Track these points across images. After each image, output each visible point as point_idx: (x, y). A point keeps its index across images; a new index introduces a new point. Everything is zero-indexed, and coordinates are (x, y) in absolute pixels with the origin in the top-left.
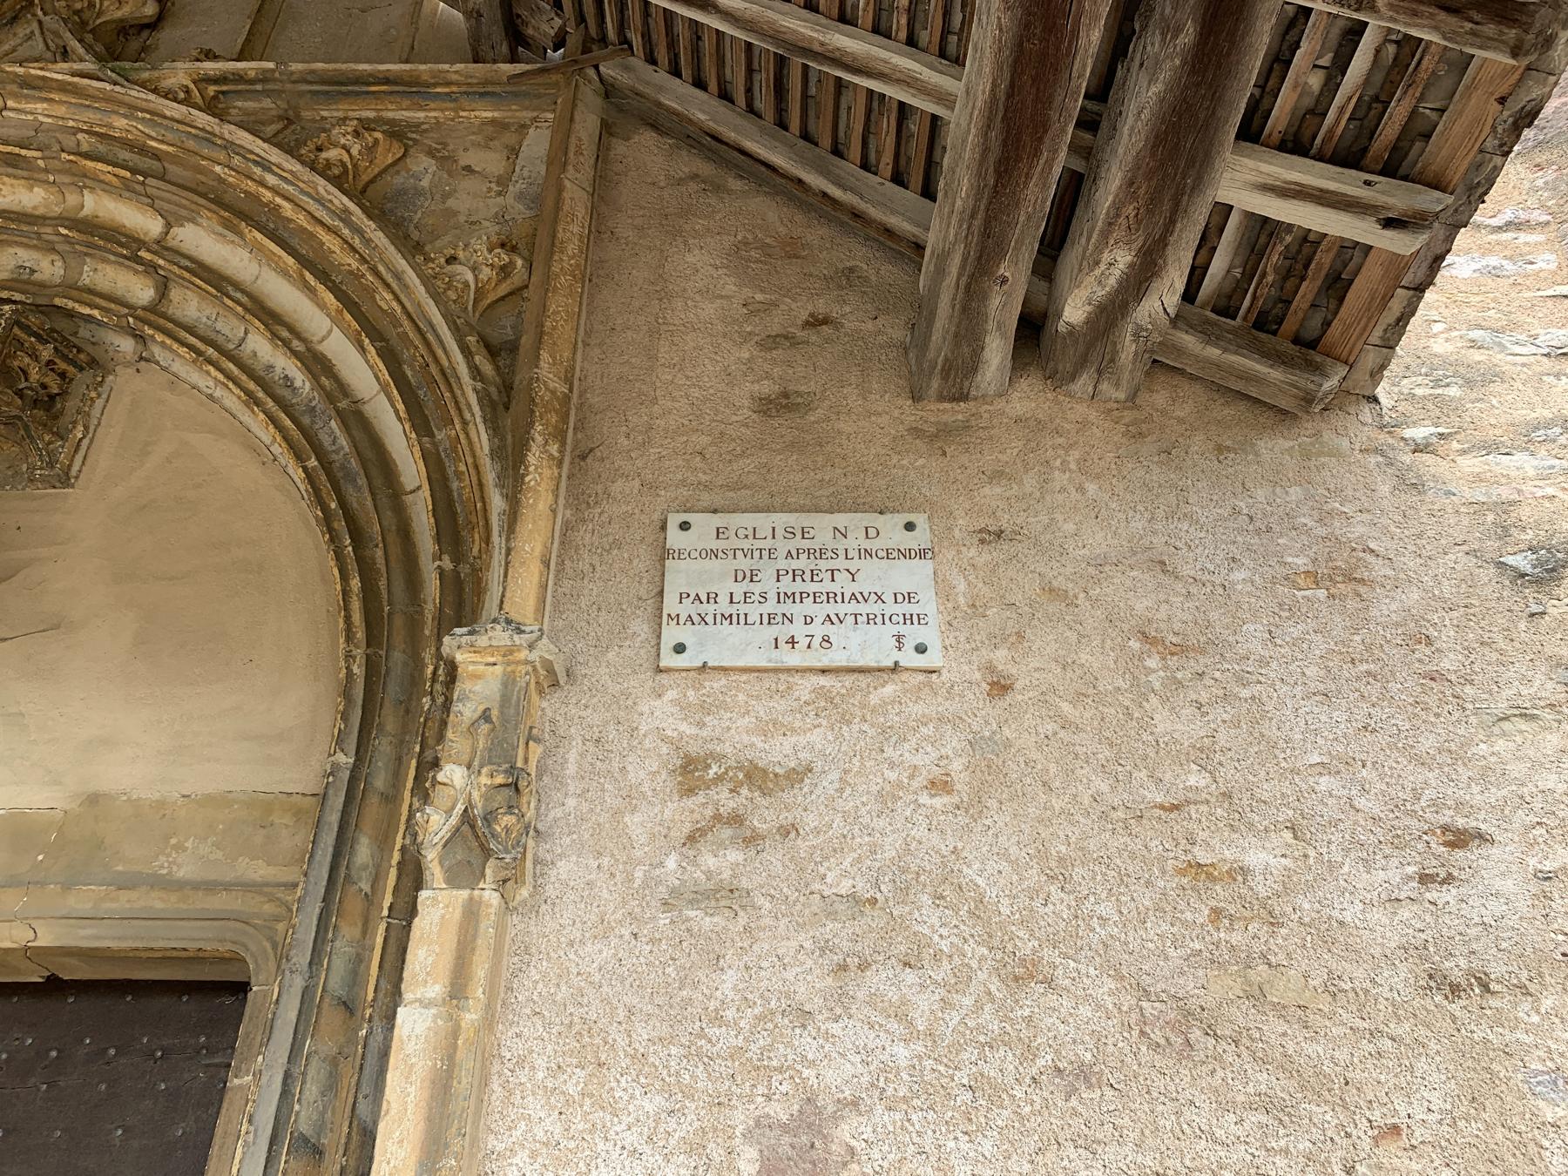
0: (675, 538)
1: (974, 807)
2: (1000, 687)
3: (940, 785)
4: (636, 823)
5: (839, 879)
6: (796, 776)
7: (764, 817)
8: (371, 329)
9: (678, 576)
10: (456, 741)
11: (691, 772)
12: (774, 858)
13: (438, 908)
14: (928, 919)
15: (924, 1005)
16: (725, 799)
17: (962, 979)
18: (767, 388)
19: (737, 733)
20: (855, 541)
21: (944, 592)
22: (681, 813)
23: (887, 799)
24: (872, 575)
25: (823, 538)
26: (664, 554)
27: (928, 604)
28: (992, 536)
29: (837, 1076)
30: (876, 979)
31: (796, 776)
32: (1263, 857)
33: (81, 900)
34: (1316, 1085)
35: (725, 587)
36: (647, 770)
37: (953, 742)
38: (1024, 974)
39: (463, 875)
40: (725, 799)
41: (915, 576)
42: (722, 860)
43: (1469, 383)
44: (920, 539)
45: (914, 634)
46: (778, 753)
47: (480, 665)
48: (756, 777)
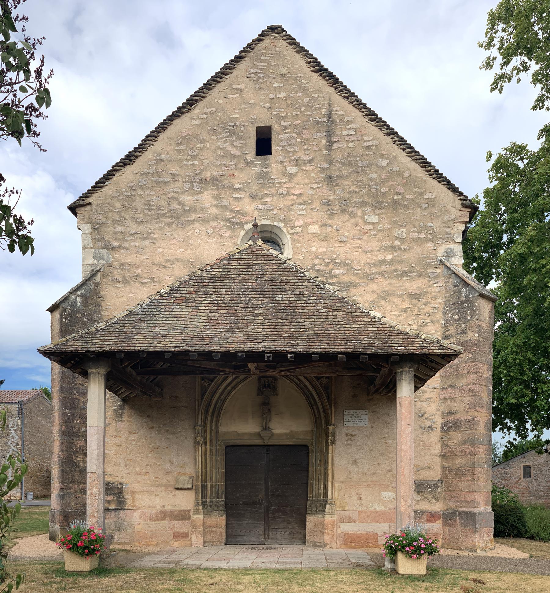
0: (345, 413)
1: (369, 438)
2: (372, 427)
3: (367, 436)
4: (343, 439)
5: (358, 443)
6: (355, 435)
7: (353, 439)
8: (313, 387)
9: (345, 417)
10: (330, 435)
11: (347, 435)
12: (353, 442)
13: (330, 447)
14: (365, 446)
15: (364, 452)
16: (349, 437)
17: (367, 451)
18: (353, 394)
19: (350, 432)
20: (361, 413)
21: (368, 418)
22: (346, 438)
23: (362, 437)
24: (363, 417)
25: (358, 413)
26: (344, 415)
27: (367, 420)
28: (373, 412)
29: (357, 457)
30: (361, 451)
31: (355, 435)
32: (390, 442)
33: (294, 440)
34: (391, 458)
35: (349, 418)
36: (343, 435)
37: (368, 432)
38: (371, 450)
39: (332, 445)
40: (349, 437)
41: (366, 417)
42: (349, 442)
43: (423, 393)
44: (367, 413)
45: (366, 423)
46: (354, 433)
47: (331, 428)
48: (352, 435)
